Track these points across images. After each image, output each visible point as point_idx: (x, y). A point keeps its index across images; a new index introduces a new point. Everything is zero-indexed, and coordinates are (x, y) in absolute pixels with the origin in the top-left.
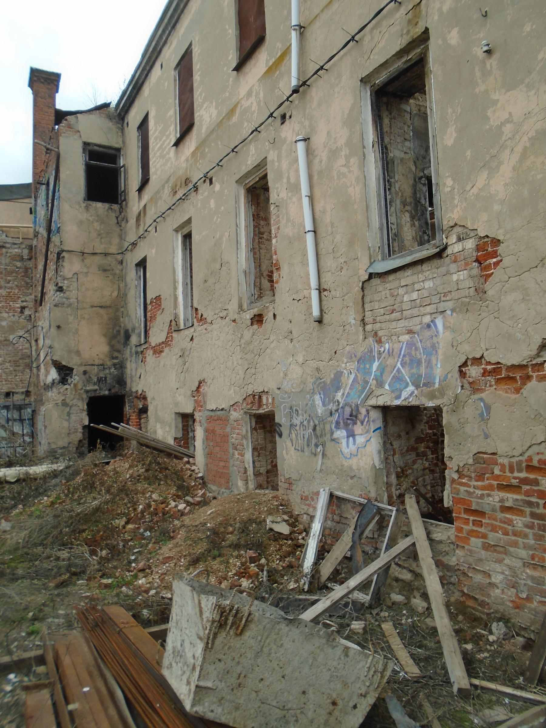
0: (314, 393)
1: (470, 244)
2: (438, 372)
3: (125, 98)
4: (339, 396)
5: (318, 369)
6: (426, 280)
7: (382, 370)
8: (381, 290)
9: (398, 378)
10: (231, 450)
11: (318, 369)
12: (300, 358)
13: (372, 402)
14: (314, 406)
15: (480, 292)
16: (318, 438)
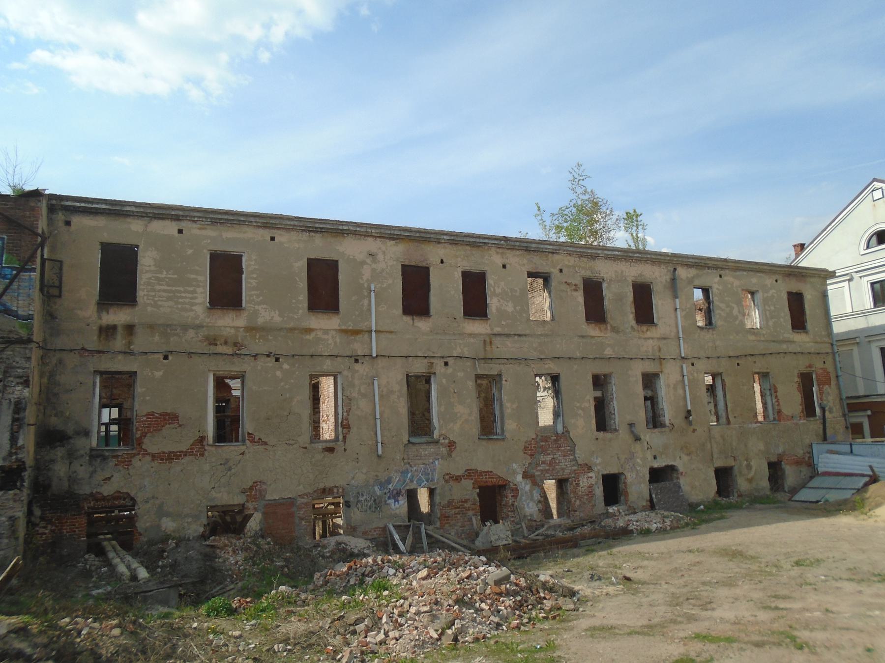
0: (374, 486)
1: (447, 441)
2: (436, 477)
3: (83, 205)
4: (390, 486)
5: (377, 476)
6: (432, 449)
7: (412, 476)
8: (414, 448)
9: (420, 479)
10: (297, 521)
11: (377, 476)
12: (364, 471)
13: (408, 488)
14: (374, 492)
15: (450, 455)
16: (378, 504)
